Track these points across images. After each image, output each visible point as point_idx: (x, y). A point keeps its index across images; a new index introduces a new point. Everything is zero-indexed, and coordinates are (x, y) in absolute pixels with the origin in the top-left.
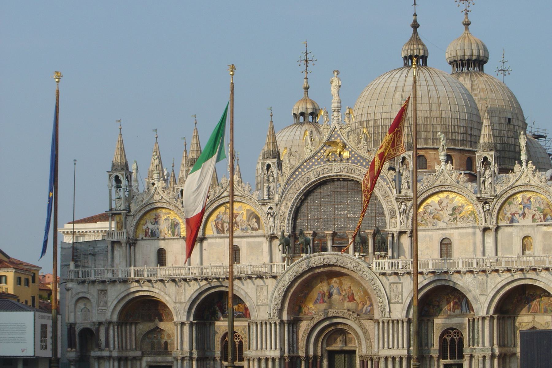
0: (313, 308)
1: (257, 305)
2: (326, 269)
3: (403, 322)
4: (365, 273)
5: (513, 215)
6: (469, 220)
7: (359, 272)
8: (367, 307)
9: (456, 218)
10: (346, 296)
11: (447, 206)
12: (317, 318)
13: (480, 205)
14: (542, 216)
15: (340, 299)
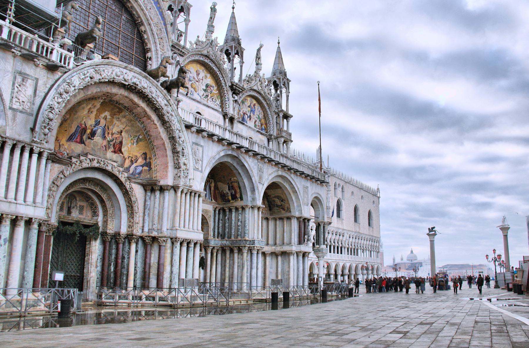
0: (66, 147)
1: (11, 108)
2: (123, 92)
3: (199, 196)
4: (173, 118)
5: (244, 114)
6: (216, 103)
7: (168, 115)
8: (137, 166)
9: (207, 96)
10: (112, 143)
11: (203, 80)
12: (77, 164)
13: (230, 93)
14: (260, 124)
15: (103, 145)
